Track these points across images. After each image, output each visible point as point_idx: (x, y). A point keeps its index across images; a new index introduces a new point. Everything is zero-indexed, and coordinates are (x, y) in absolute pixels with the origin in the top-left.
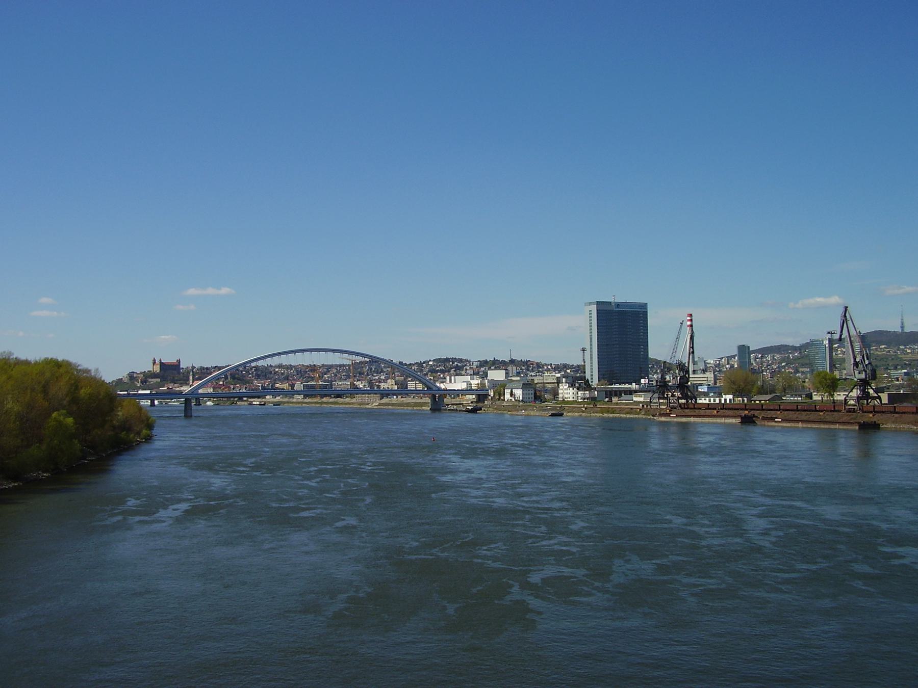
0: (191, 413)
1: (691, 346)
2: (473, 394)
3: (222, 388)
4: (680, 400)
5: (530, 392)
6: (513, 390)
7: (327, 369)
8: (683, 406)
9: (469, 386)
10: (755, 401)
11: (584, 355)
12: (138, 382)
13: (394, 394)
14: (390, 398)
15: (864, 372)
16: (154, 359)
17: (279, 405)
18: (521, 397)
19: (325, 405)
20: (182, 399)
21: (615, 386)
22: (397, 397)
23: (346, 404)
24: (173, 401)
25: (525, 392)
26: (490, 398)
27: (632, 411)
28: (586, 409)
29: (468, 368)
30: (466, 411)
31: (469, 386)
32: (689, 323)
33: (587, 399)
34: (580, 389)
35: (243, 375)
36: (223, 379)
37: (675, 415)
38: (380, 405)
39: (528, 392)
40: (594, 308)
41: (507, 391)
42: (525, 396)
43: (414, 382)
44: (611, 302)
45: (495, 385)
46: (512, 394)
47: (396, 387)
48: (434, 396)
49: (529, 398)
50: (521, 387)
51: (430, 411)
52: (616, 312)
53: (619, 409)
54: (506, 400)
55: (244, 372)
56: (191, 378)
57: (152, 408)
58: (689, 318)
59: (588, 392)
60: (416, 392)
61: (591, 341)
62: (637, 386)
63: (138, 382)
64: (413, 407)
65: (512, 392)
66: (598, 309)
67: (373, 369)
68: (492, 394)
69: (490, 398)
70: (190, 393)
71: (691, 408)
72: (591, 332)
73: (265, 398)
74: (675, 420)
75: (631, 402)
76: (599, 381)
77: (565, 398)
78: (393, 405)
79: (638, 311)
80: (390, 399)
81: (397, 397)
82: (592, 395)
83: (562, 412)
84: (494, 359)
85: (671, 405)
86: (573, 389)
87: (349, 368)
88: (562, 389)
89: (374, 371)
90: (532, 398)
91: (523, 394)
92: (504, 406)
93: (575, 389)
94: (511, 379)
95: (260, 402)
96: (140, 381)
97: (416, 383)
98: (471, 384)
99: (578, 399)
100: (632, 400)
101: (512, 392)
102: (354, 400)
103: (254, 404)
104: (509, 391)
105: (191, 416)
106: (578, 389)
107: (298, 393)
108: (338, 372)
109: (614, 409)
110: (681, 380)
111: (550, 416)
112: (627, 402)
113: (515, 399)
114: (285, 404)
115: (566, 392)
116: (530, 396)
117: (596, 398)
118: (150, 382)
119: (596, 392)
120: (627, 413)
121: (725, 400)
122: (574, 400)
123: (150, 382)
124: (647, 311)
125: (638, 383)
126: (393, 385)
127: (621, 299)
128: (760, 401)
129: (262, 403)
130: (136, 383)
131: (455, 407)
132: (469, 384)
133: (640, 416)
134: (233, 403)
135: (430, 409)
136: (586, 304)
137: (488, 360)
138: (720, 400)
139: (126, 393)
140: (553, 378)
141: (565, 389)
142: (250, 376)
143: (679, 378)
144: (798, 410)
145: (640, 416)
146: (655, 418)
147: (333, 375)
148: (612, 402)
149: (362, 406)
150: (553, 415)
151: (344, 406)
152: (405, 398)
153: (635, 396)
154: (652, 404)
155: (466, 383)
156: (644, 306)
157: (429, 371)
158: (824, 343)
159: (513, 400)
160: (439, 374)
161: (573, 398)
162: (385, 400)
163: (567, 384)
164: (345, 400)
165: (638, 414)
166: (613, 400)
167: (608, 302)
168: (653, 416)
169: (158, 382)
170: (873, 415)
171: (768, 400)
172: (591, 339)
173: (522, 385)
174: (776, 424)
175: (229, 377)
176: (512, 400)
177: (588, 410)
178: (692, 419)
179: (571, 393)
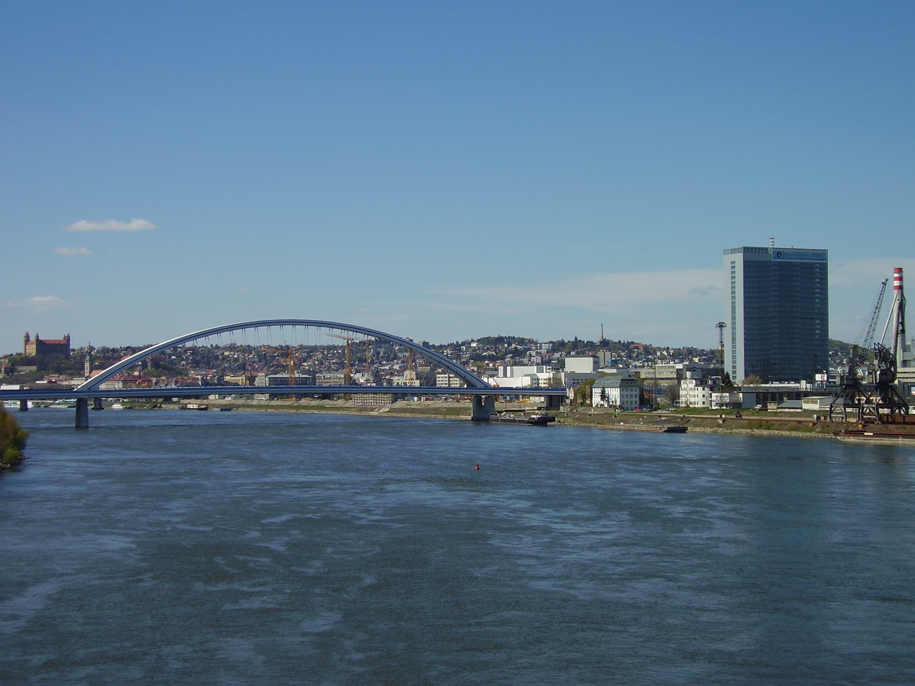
0: (88, 423)
1: (900, 321)
2: (540, 396)
3: (138, 382)
4: (880, 409)
5: (634, 393)
6: (606, 389)
8: (885, 419)
9: (534, 381)
13: (414, 395)
16: (27, 333)
17: (230, 410)
18: (618, 400)
19: (304, 411)
20: (72, 400)
21: (772, 385)
24: (57, 402)
25: (625, 393)
26: (568, 401)
28: (723, 421)
29: (534, 353)
30: (529, 422)
31: (534, 381)
32: (896, 283)
33: (727, 405)
34: (716, 389)
35: (172, 361)
36: (139, 368)
37: (872, 434)
39: (629, 393)
40: (739, 258)
41: (596, 392)
42: (625, 400)
43: (447, 376)
44: (766, 249)
45: (576, 381)
46: (603, 396)
47: (417, 383)
48: (478, 399)
51: (472, 422)
54: (594, 406)
55: (174, 357)
56: (87, 365)
58: (896, 275)
59: (727, 394)
60: (450, 391)
62: (809, 386)
64: (446, 414)
65: (603, 392)
66: (745, 259)
67: (382, 354)
68: (571, 394)
69: (568, 401)
71: (899, 423)
72: (734, 298)
73: (208, 398)
75: (800, 410)
76: (746, 376)
78: (413, 411)
79: (812, 263)
80: (407, 402)
82: (735, 399)
83: (685, 426)
85: (865, 417)
86: (704, 389)
87: (343, 352)
88: (685, 389)
89: (382, 357)
90: (636, 402)
91: (622, 396)
92: (590, 415)
94: (603, 372)
96: (3, 369)
97: (449, 377)
98: (538, 379)
99: (711, 406)
100: (801, 408)
101: (603, 392)
102: (350, 404)
104: (599, 390)
106: (712, 390)
107: (261, 390)
112: (792, 410)
113: (608, 404)
114: (240, 409)
115: (692, 393)
116: (634, 399)
119: (741, 395)
120: (790, 429)
122: (705, 406)
124: (826, 264)
125: (811, 380)
129: (203, 407)
131: (512, 415)
132: (536, 380)
133: (814, 434)
134: (156, 406)
136: (726, 252)
140: (671, 370)
141: (691, 389)
142: (184, 362)
143: (878, 373)
145: (814, 434)
147: (317, 362)
148: (767, 410)
149: (363, 413)
150: (670, 430)
151: (334, 412)
152: (433, 400)
153: (805, 402)
154: (832, 415)
155: (529, 377)
156: (821, 255)
157: (471, 358)
159: (606, 405)
160: (486, 362)
161: (704, 403)
162: (400, 404)
163: (694, 381)
164: (335, 403)
165: (810, 431)
167: (763, 248)
168: (835, 434)
169: (34, 372)
172: (733, 308)
173: (620, 380)
175: (149, 365)
176: (603, 405)
177: (727, 423)
178: (900, 441)
179: (700, 396)
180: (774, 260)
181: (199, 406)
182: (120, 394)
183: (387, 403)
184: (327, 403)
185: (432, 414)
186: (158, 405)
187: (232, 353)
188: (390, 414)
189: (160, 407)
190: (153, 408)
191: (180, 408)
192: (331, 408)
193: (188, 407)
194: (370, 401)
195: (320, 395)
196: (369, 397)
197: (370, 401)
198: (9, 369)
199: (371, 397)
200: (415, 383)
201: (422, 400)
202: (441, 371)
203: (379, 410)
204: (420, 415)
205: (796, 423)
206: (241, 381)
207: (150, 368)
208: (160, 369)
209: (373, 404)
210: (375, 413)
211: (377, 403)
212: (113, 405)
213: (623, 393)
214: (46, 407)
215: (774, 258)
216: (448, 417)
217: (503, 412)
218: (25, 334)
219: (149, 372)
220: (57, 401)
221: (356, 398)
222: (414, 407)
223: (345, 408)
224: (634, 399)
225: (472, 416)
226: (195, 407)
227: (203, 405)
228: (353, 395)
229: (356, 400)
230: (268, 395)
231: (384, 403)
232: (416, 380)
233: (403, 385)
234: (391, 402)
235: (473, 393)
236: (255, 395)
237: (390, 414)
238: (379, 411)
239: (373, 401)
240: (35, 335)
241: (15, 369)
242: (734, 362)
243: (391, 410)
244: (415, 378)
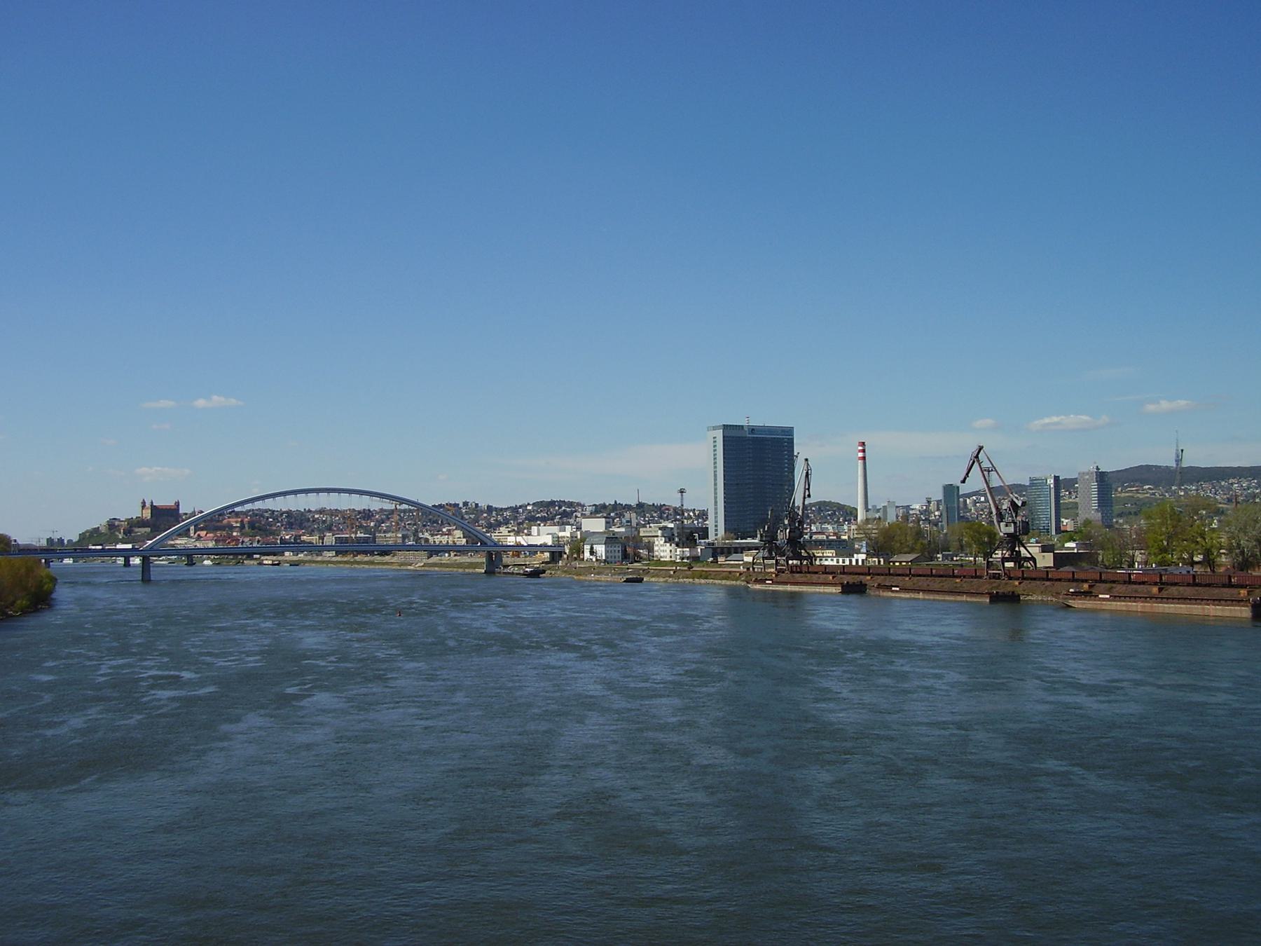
0: (150, 577)
1: (807, 487)
4: (765, 561)
5: (617, 549)
6: (595, 546)
7: (387, 515)
8: (795, 570)
10: (894, 562)
11: (682, 499)
12: (120, 533)
13: (446, 552)
14: (441, 556)
15: (1012, 524)
16: (144, 500)
17: (297, 565)
18: (604, 554)
19: (356, 566)
20: (173, 557)
22: (450, 555)
23: (387, 563)
24: (161, 559)
25: (610, 549)
26: (565, 556)
27: (730, 576)
28: (674, 572)
29: (579, 515)
32: (861, 455)
33: (688, 558)
36: (237, 529)
40: (719, 434)
41: (587, 548)
42: (609, 554)
44: (742, 426)
46: (592, 552)
48: (490, 555)
49: (615, 557)
50: (604, 542)
52: (749, 439)
53: (714, 573)
54: (585, 559)
55: (271, 520)
57: (127, 569)
58: (860, 448)
59: (688, 549)
61: (715, 480)
63: (120, 533)
65: (592, 548)
69: (565, 556)
71: (805, 572)
72: (715, 467)
73: (284, 555)
74: (771, 588)
75: (741, 562)
76: (725, 532)
77: (661, 557)
78: (441, 565)
81: (450, 555)
84: (616, 502)
86: (671, 545)
88: (658, 545)
90: (619, 557)
91: (607, 551)
93: (673, 545)
94: (151, 540)
95: (273, 561)
96: (122, 531)
100: (743, 560)
101: (592, 548)
102: (395, 559)
104: (589, 547)
107: (329, 548)
108: (401, 519)
109: (708, 573)
110: (792, 534)
111: (625, 581)
115: (662, 548)
116: (617, 554)
117: (699, 557)
121: (857, 561)
122: (672, 559)
126: (460, 538)
127: (756, 422)
128: (900, 562)
129: (276, 562)
130: (117, 533)
131: (516, 569)
133: (738, 583)
134: (239, 563)
137: (607, 504)
138: (851, 561)
139: (100, 547)
142: (279, 524)
143: (788, 531)
144: (890, 574)
145: (738, 583)
146: (749, 585)
149: (402, 567)
150: (628, 581)
151: (380, 567)
152: (460, 556)
153: (746, 556)
156: (789, 432)
157: (526, 519)
158: (1048, 482)
159: (594, 560)
160: (539, 522)
161: (671, 557)
162: (435, 559)
163: (663, 539)
165: (736, 580)
166: (719, 560)
167: (739, 426)
170: (1020, 583)
171: (911, 561)
172: (715, 476)
174: (893, 595)
175: (246, 526)
179: (668, 551)
180: (750, 436)
187: (322, 516)
188: (423, 568)
189: (243, 562)
192: (378, 564)
205: (727, 573)
210: (412, 567)
213: (607, 549)
215: (749, 434)
216: (467, 570)
218: (141, 501)
222: (444, 562)
224: (617, 554)
241: (133, 530)
242: (716, 522)
244: (462, 536)
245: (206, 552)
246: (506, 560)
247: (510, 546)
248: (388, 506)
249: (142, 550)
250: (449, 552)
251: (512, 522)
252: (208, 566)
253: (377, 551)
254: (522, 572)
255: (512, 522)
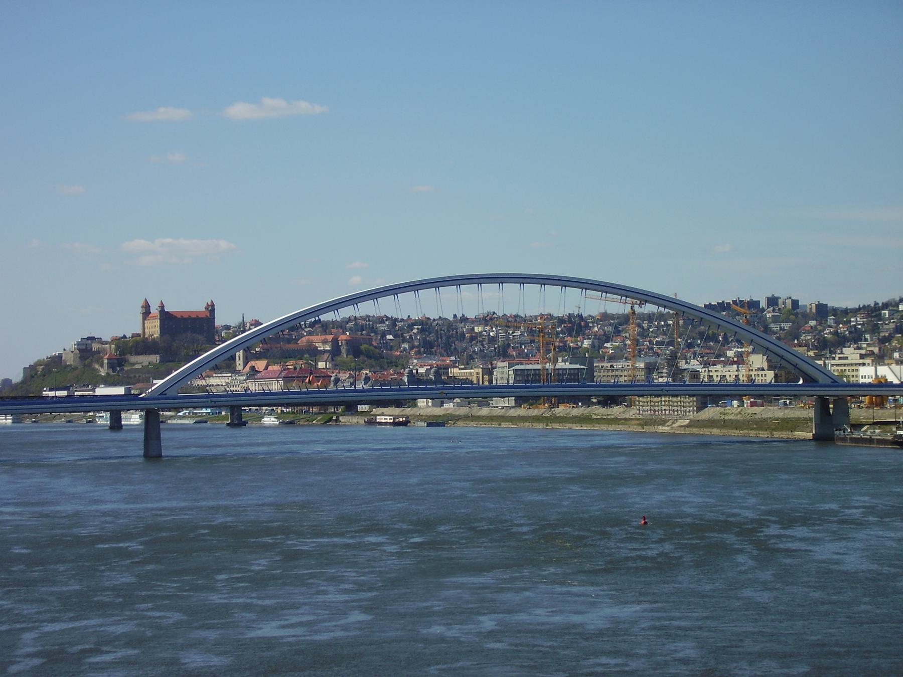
3: (307, 380)
12: (102, 366)
13: (733, 397)
17: (442, 425)
19: (556, 426)
20: (204, 411)
22: (742, 404)
23: (616, 421)
24: (181, 414)
30: (893, 443)
35: (388, 346)
36: (326, 356)
38: (693, 424)
47: (770, 376)
48: (822, 403)
51: (813, 443)
55: (390, 337)
63: (102, 366)
64: (773, 430)
70: (156, 395)
73: (416, 406)
78: (725, 424)
80: (722, 410)
81: (742, 404)
95: (395, 417)
96: (106, 361)
102: (632, 413)
103: (380, 423)
105: (160, 456)
107: (502, 391)
108: (644, 334)
114: (460, 423)
118: (134, 364)
123: (134, 364)
126: (763, 370)
129: (401, 420)
130: (97, 366)
131: (877, 431)
134: (330, 420)
135: (816, 438)
139: (64, 393)
142: (406, 345)
147: (628, 342)
162: (711, 412)
169: (155, 365)
175: (343, 350)
181: (394, 419)
182: (211, 401)
183: (689, 412)
184: (596, 412)
185: (752, 429)
186: (334, 418)
187: (488, 328)
188: (688, 431)
189: (337, 420)
190: (326, 422)
191: (365, 421)
192: (599, 421)
193: (378, 420)
194: (664, 408)
195: (601, 399)
196: (661, 401)
197: (664, 408)
198: (116, 361)
199: (665, 401)
200: (765, 375)
201: (745, 406)
202: (813, 355)
203: (673, 423)
204: (735, 431)
206: (475, 375)
207: (345, 356)
208: (362, 358)
209: (667, 412)
211: (673, 411)
212: (263, 417)
214: (69, 422)
217: (865, 425)
219: (344, 362)
220: (180, 412)
221: (641, 403)
222: (731, 417)
223: (621, 419)
225: (814, 433)
226: (389, 421)
227: (402, 416)
228: (637, 399)
229: (642, 406)
230: (514, 398)
231: (685, 411)
232: (768, 370)
233: (706, 380)
234: (695, 408)
235: (813, 393)
236: (494, 398)
237: (688, 431)
238: (674, 425)
239: (667, 408)
240: (159, 304)
241: (126, 361)
243: (693, 423)
244: (766, 367)
245: (268, 400)
246: (857, 413)
247: (864, 385)
248: (617, 307)
249: (143, 399)
250: (739, 398)
251: (868, 336)
252: (269, 427)
253: (597, 396)
254: (889, 437)
255: (868, 336)
